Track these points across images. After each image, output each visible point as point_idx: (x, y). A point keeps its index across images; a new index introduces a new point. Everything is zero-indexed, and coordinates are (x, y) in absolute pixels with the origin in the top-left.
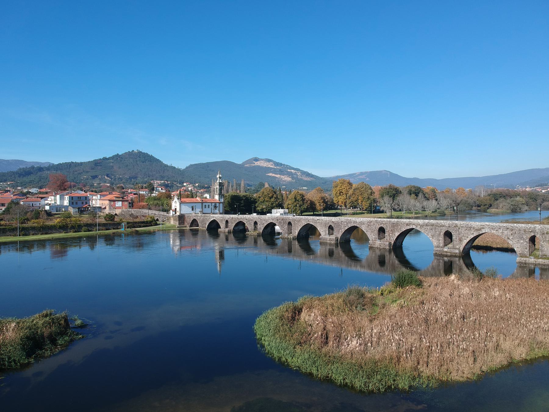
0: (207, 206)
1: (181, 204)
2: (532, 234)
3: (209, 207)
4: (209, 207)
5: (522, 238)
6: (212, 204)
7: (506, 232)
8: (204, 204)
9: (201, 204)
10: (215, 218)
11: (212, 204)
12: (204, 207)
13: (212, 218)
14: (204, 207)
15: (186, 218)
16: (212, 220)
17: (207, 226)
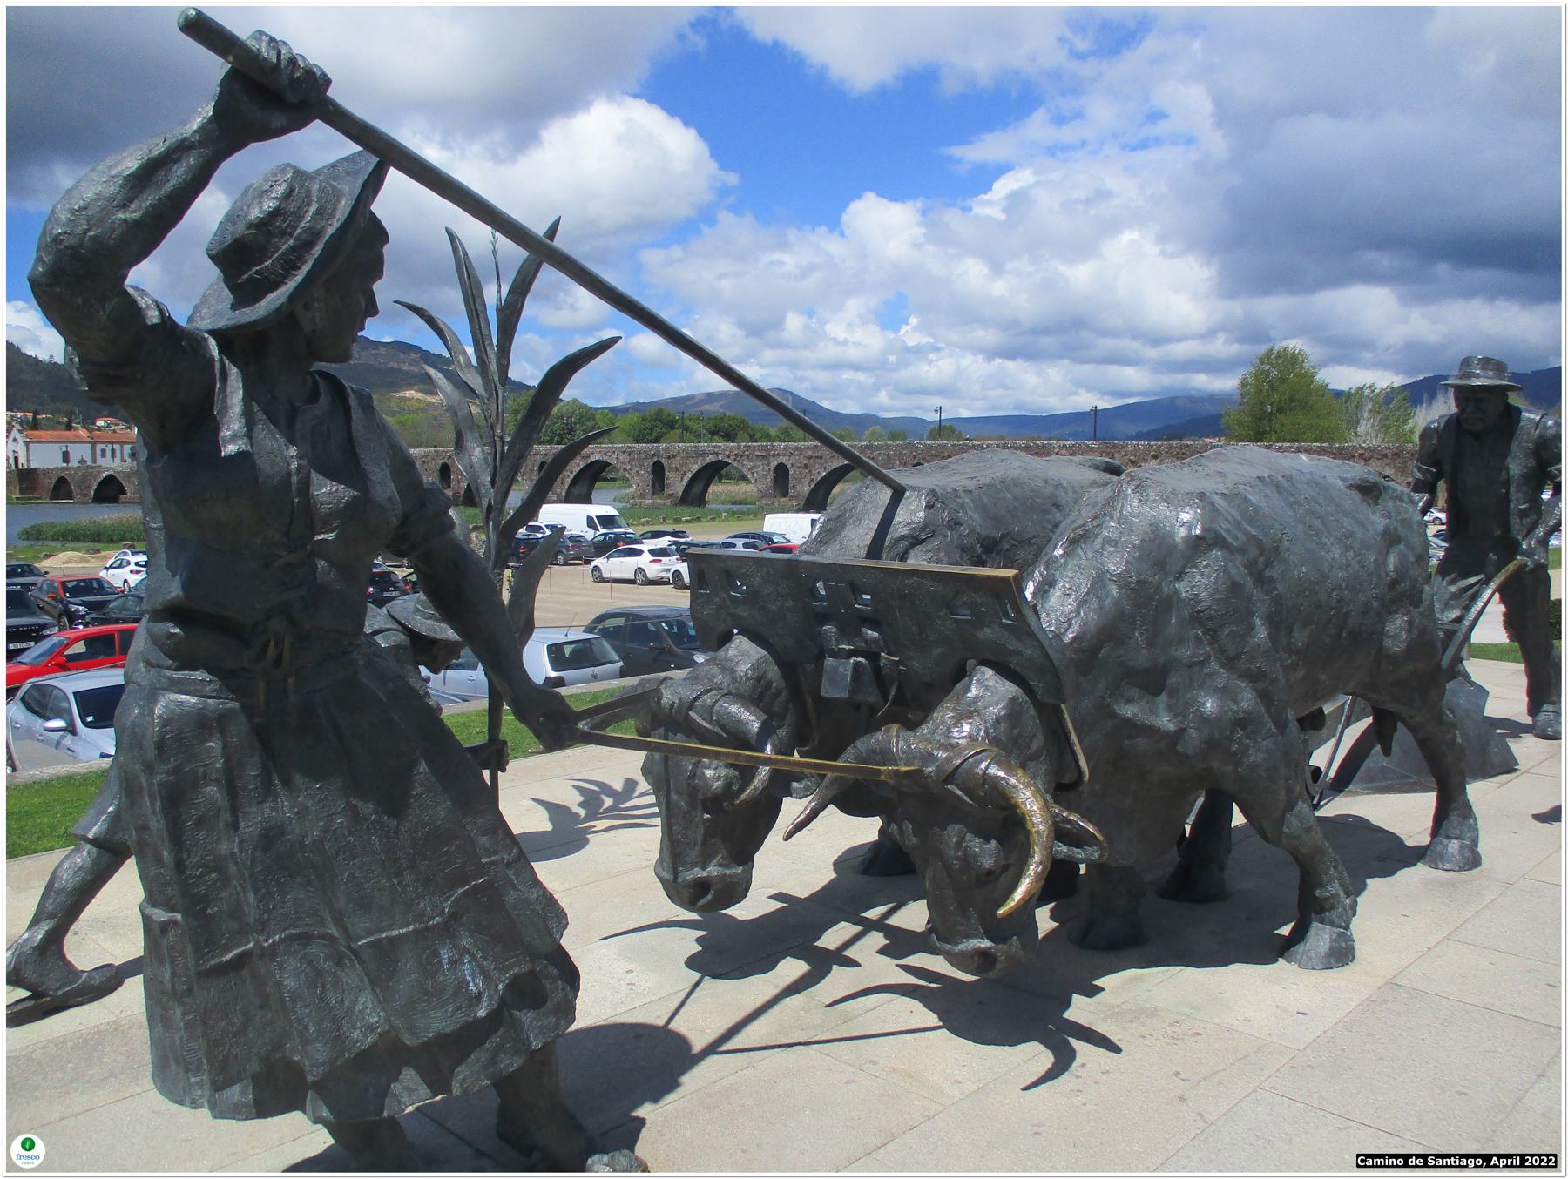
0: (109, 453)
1: (31, 445)
2: (656, 459)
3: (113, 455)
4: (113, 455)
5: (641, 466)
6: (122, 447)
7: (621, 457)
8: (99, 447)
9: (90, 445)
10: (111, 472)
11: (122, 447)
12: (99, 453)
13: (104, 472)
14: (99, 453)
15: (41, 476)
16: (106, 477)
17: (92, 492)
